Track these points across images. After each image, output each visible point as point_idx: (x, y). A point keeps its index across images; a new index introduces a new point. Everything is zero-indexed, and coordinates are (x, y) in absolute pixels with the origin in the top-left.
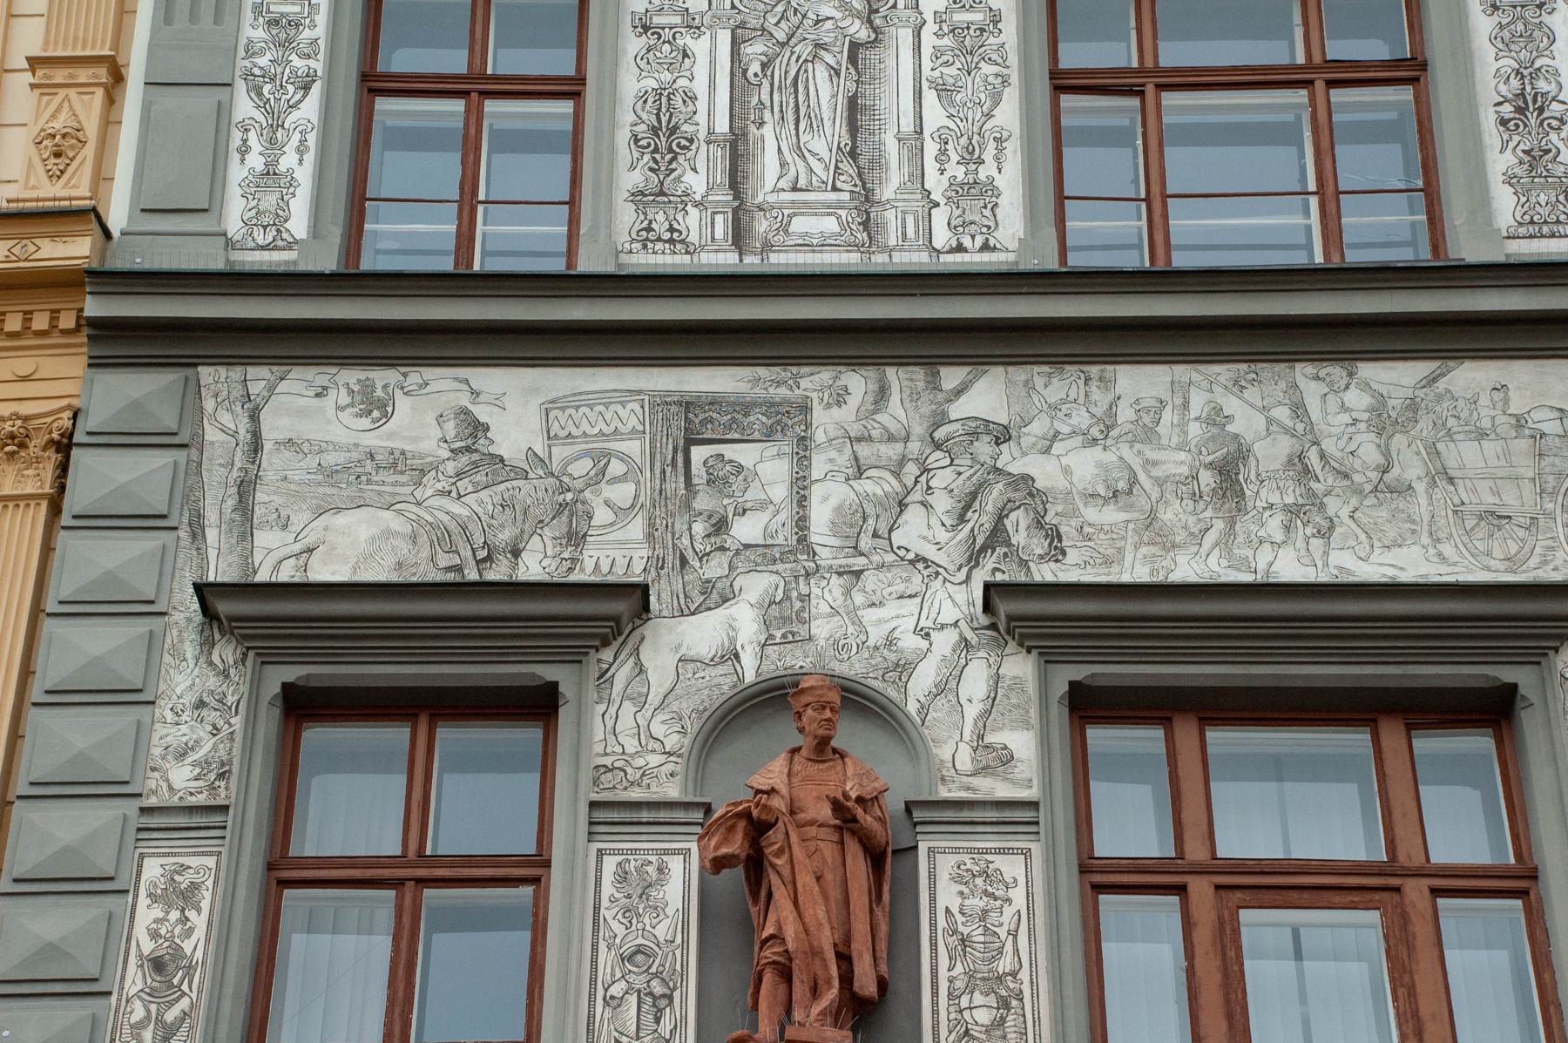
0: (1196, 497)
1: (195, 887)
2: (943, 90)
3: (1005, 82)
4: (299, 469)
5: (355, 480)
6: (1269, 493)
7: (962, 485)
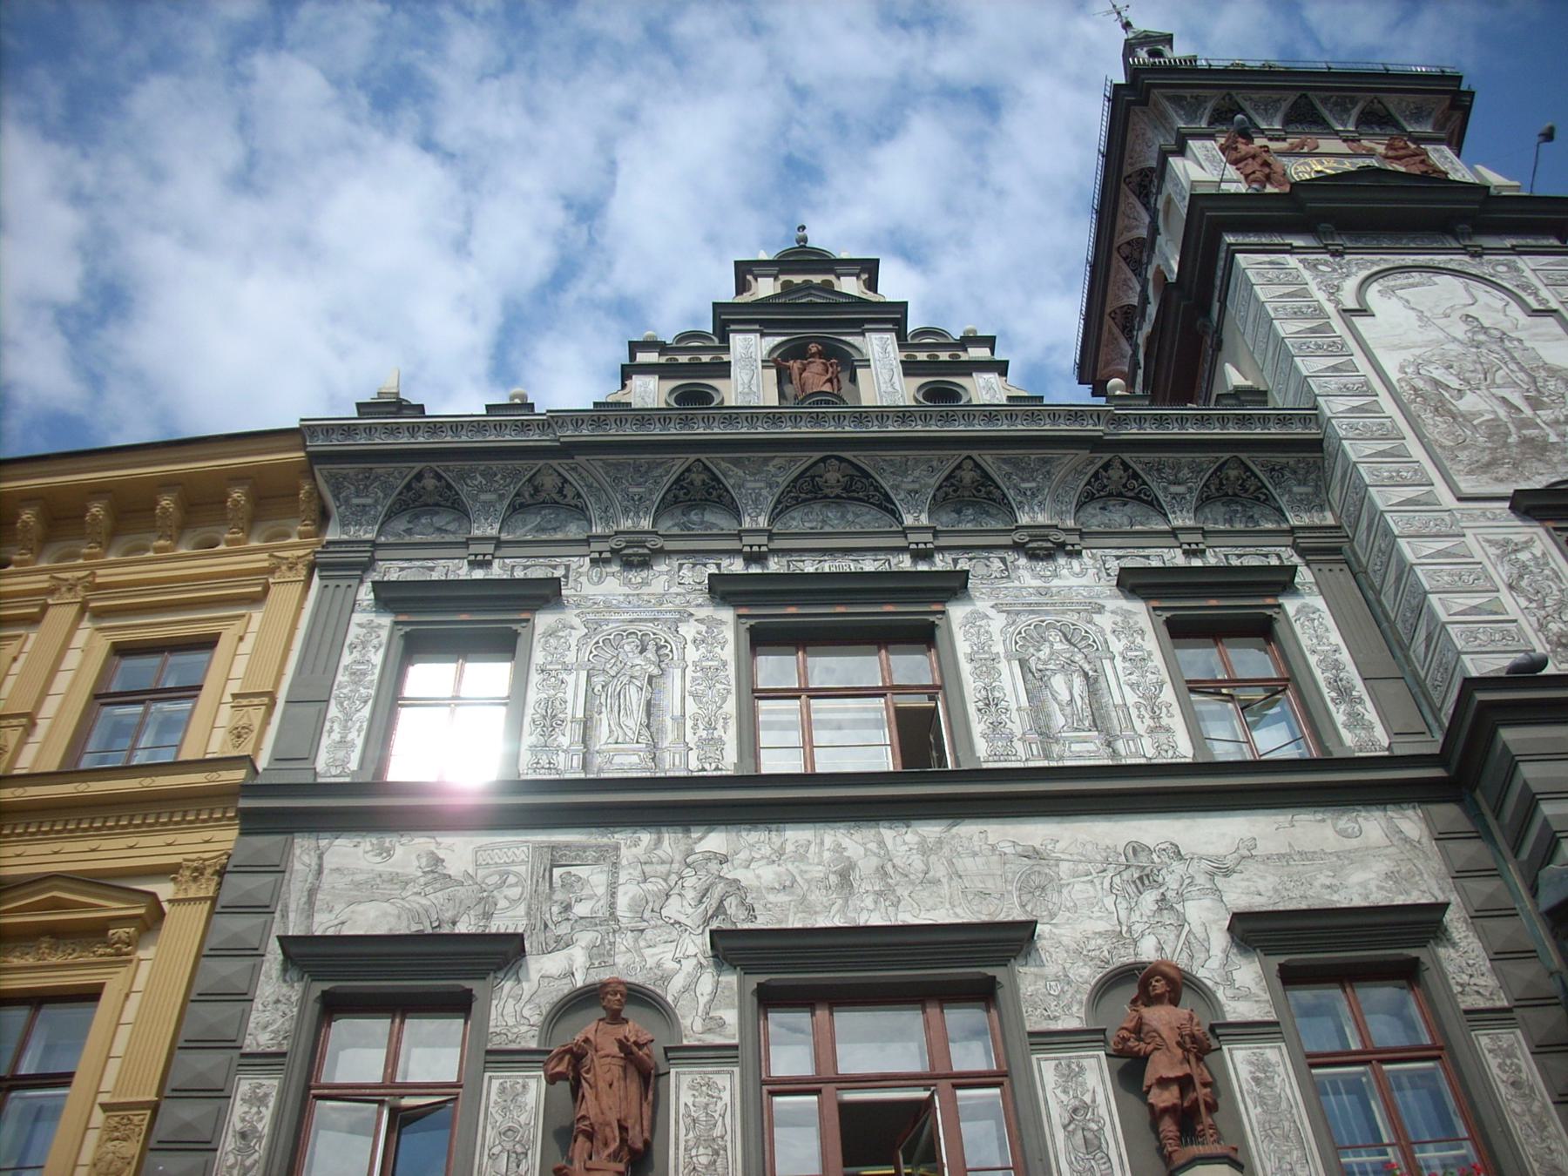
0: (828, 888)
1: (266, 1095)
2: (695, 696)
3: (729, 692)
4: (341, 882)
6: (866, 885)
7: (701, 886)
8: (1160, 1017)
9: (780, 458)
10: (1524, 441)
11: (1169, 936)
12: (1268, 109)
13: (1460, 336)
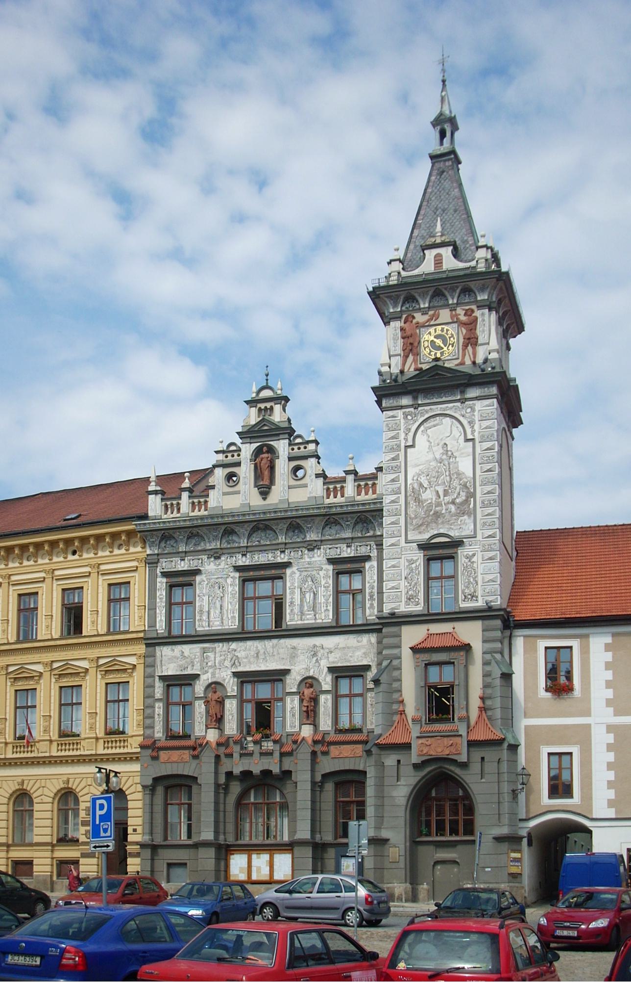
5: (172, 659)
6: (261, 657)
8: (308, 692)
9: (246, 525)
10: (436, 513)
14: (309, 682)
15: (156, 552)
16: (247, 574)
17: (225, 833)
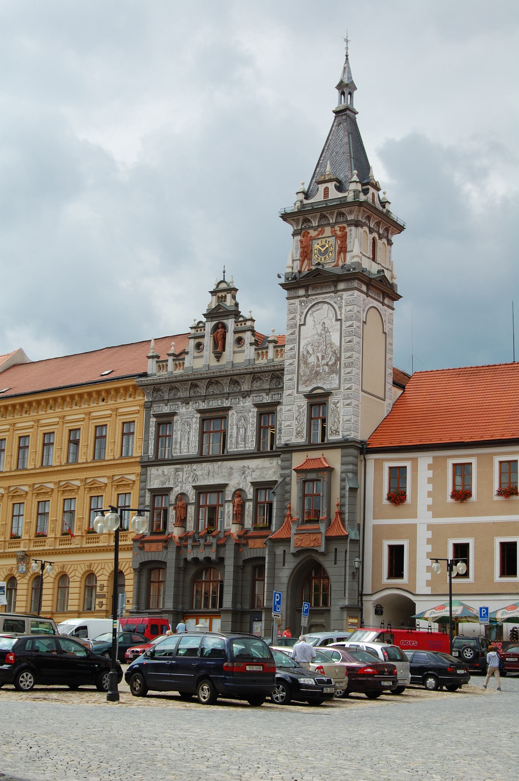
6: (211, 475)
8: (237, 500)
9: (204, 380)
10: (316, 372)
11: (244, 483)
12: (314, 217)
13: (319, 332)
14: (239, 493)
15: (151, 400)
16: (207, 415)
17: (183, 603)
